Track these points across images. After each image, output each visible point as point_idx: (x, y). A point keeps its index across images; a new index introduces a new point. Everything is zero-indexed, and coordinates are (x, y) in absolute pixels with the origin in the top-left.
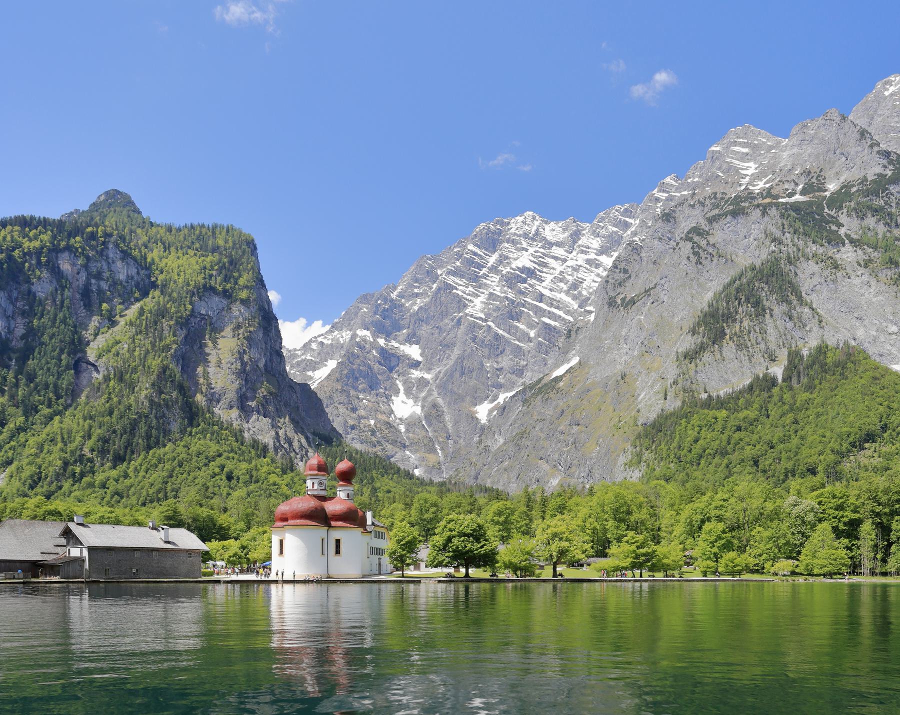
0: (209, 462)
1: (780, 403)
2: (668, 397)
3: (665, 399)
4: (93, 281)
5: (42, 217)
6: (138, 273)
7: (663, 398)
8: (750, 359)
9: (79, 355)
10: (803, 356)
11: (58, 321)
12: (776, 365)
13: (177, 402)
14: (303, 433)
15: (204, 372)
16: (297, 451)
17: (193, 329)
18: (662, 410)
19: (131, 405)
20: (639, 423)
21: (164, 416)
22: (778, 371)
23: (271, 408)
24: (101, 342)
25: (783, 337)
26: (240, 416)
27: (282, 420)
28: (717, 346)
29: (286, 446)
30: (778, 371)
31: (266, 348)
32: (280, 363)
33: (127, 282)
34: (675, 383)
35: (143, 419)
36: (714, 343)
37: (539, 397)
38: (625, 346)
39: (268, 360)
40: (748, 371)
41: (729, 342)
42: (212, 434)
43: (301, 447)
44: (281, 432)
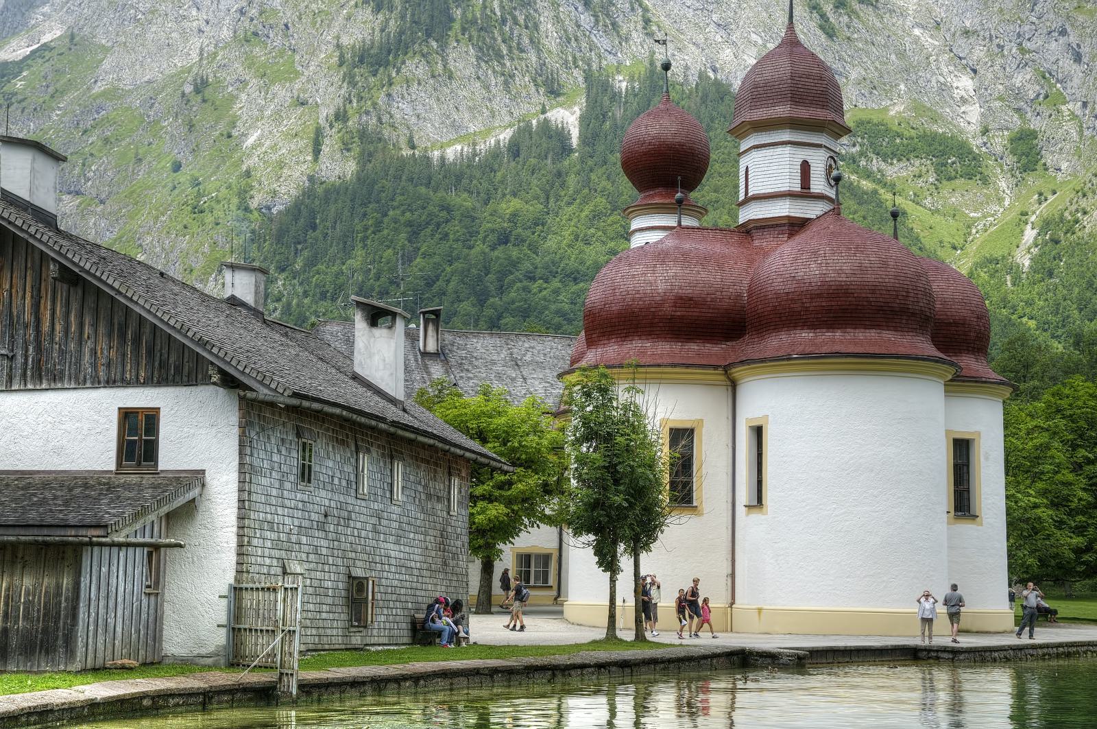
1: (586, 191)
2: (325, 149)
3: (317, 152)
8: (506, 83)
10: (620, 93)
12: (561, 105)
18: (311, 179)
20: (254, 204)
22: (568, 117)
25: (574, 44)
28: (434, 44)
30: (568, 117)
34: (340, 116)
36: (428, 34)
38: (194, 12)
40: (504, 111)
41: (460, 37)
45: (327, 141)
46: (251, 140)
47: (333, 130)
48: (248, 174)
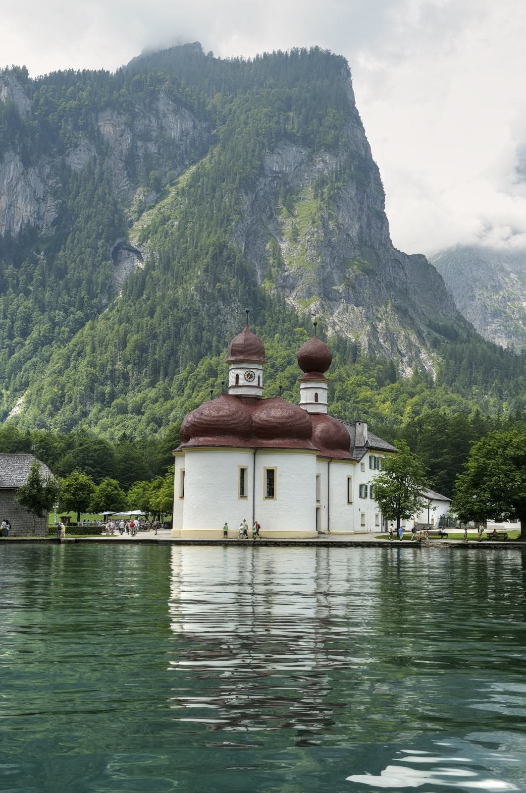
0: (276, 372)
4: (140, 144)
5: (81, 70)
6: (194, 127)
9: (119, 241)
11: (96, 199)
13: (236, 292)
14: (412, 324)
15: (274, 249)
16: (404, 352)
17: (262, 193)
19: (177, 300)
21: (219, 311)
23: (367, 292)
24: (147, 219)
26: (322, 306)
27: (382, 309)
29: (387, 345)
31: (361, 209)
32: (382, 228)
33: (181, 140)
35: (193, 319)
39: (364, 226)
42: (283, 333)
43: (410, 345)
44: (380, 326)
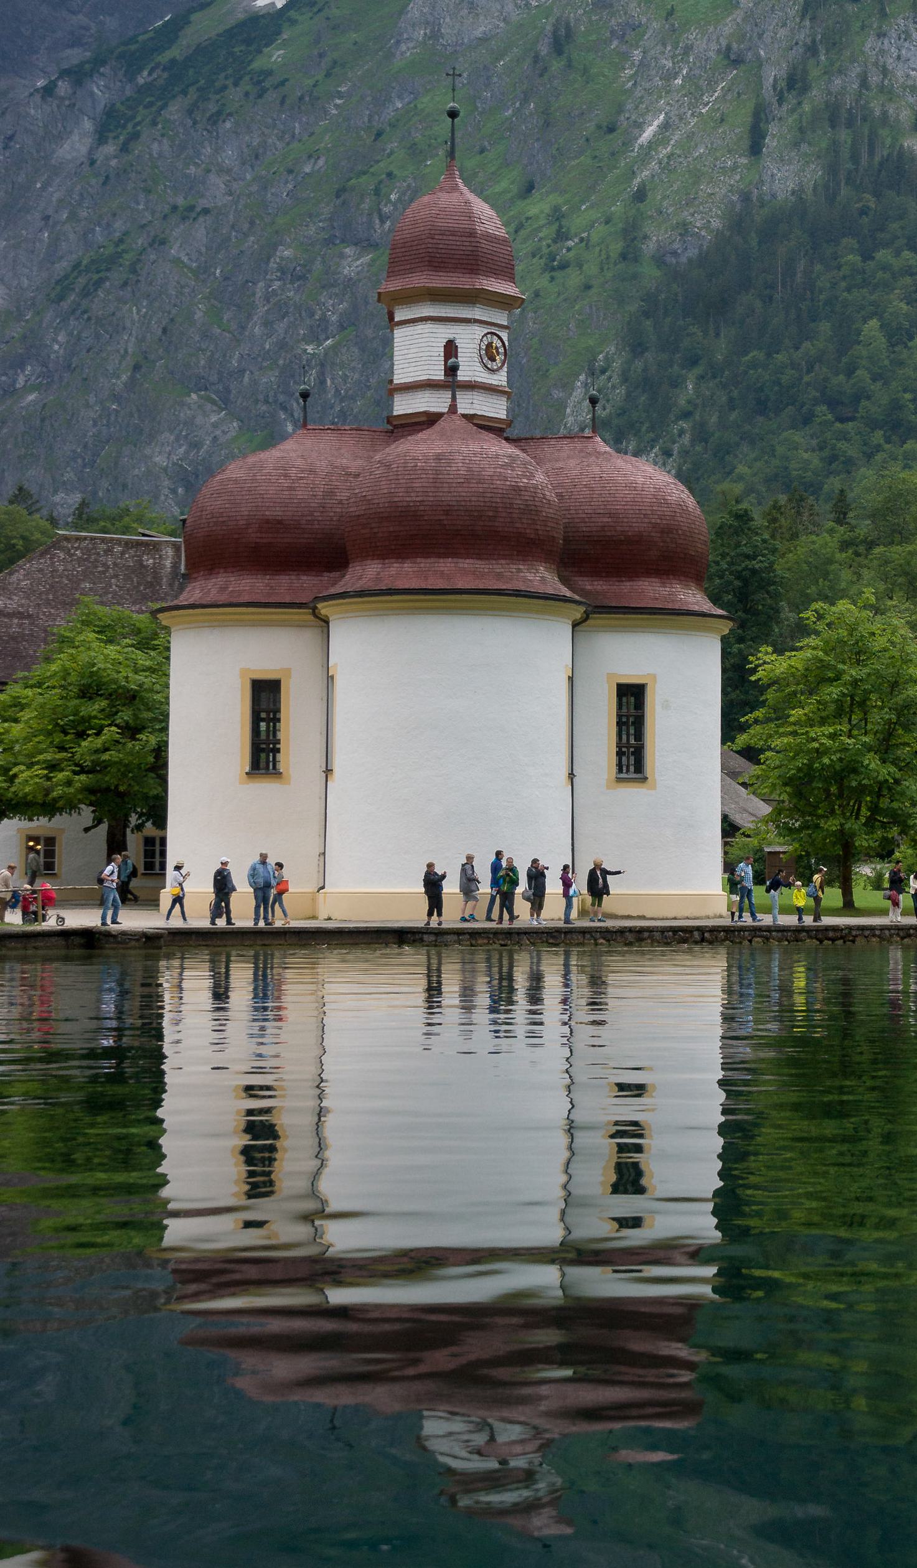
3: (755, 148)
7: (746, 143)
18: (746, 197)
37: (174, 110)
45: (773, 129)
46: (648, 133)
47: (785, 108)
48: (640, 195)
